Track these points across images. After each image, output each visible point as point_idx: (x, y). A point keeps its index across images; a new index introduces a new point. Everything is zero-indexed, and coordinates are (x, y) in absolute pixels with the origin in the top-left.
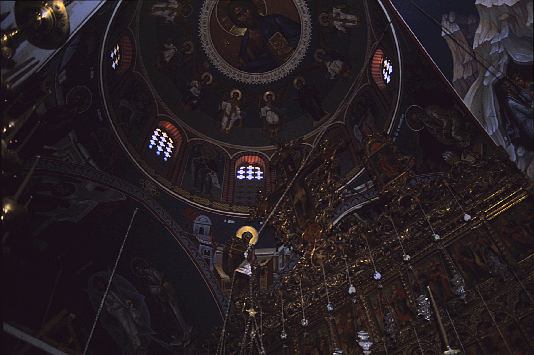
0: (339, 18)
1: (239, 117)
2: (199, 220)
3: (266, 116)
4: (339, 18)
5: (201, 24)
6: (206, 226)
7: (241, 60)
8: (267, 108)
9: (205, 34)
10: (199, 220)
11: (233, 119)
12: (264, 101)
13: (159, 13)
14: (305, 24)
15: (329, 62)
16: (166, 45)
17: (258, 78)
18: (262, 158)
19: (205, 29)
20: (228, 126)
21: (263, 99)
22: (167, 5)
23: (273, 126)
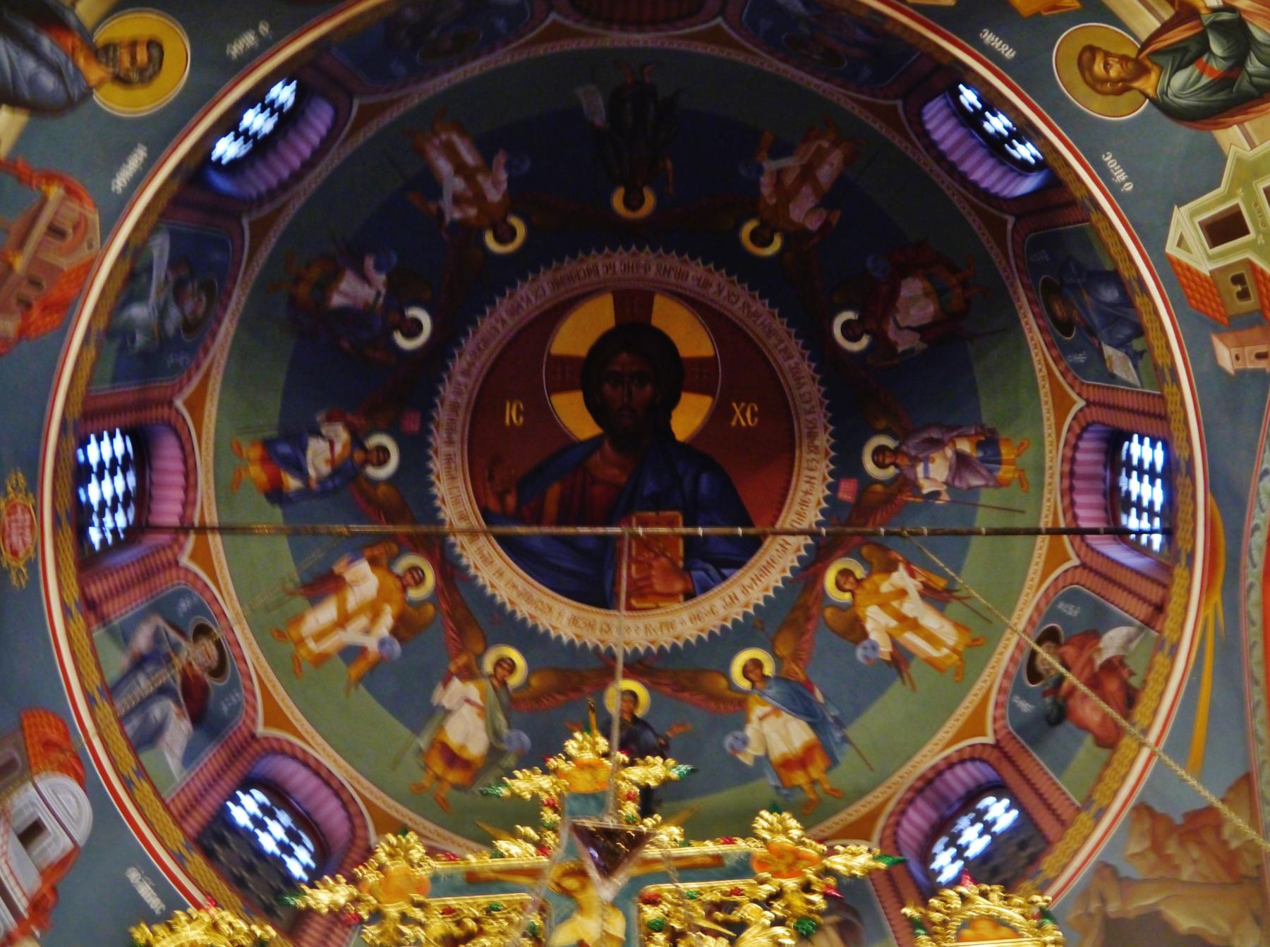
0: (895, 604)
3: (448, 713)
4: (895, 604)
5: (503, 306)
7: (511, 501)
8: (473, 691)
9: (486, 342)
11: (352, 635)
13: (444, 166)
14: (774, 553)
15: (767, 709)
16: (369, 262)
17: (514, 586)
19: (499, 326)
20: (320, 636)
21: (479, 658)
22: (477, 170)
23: (452, 758)
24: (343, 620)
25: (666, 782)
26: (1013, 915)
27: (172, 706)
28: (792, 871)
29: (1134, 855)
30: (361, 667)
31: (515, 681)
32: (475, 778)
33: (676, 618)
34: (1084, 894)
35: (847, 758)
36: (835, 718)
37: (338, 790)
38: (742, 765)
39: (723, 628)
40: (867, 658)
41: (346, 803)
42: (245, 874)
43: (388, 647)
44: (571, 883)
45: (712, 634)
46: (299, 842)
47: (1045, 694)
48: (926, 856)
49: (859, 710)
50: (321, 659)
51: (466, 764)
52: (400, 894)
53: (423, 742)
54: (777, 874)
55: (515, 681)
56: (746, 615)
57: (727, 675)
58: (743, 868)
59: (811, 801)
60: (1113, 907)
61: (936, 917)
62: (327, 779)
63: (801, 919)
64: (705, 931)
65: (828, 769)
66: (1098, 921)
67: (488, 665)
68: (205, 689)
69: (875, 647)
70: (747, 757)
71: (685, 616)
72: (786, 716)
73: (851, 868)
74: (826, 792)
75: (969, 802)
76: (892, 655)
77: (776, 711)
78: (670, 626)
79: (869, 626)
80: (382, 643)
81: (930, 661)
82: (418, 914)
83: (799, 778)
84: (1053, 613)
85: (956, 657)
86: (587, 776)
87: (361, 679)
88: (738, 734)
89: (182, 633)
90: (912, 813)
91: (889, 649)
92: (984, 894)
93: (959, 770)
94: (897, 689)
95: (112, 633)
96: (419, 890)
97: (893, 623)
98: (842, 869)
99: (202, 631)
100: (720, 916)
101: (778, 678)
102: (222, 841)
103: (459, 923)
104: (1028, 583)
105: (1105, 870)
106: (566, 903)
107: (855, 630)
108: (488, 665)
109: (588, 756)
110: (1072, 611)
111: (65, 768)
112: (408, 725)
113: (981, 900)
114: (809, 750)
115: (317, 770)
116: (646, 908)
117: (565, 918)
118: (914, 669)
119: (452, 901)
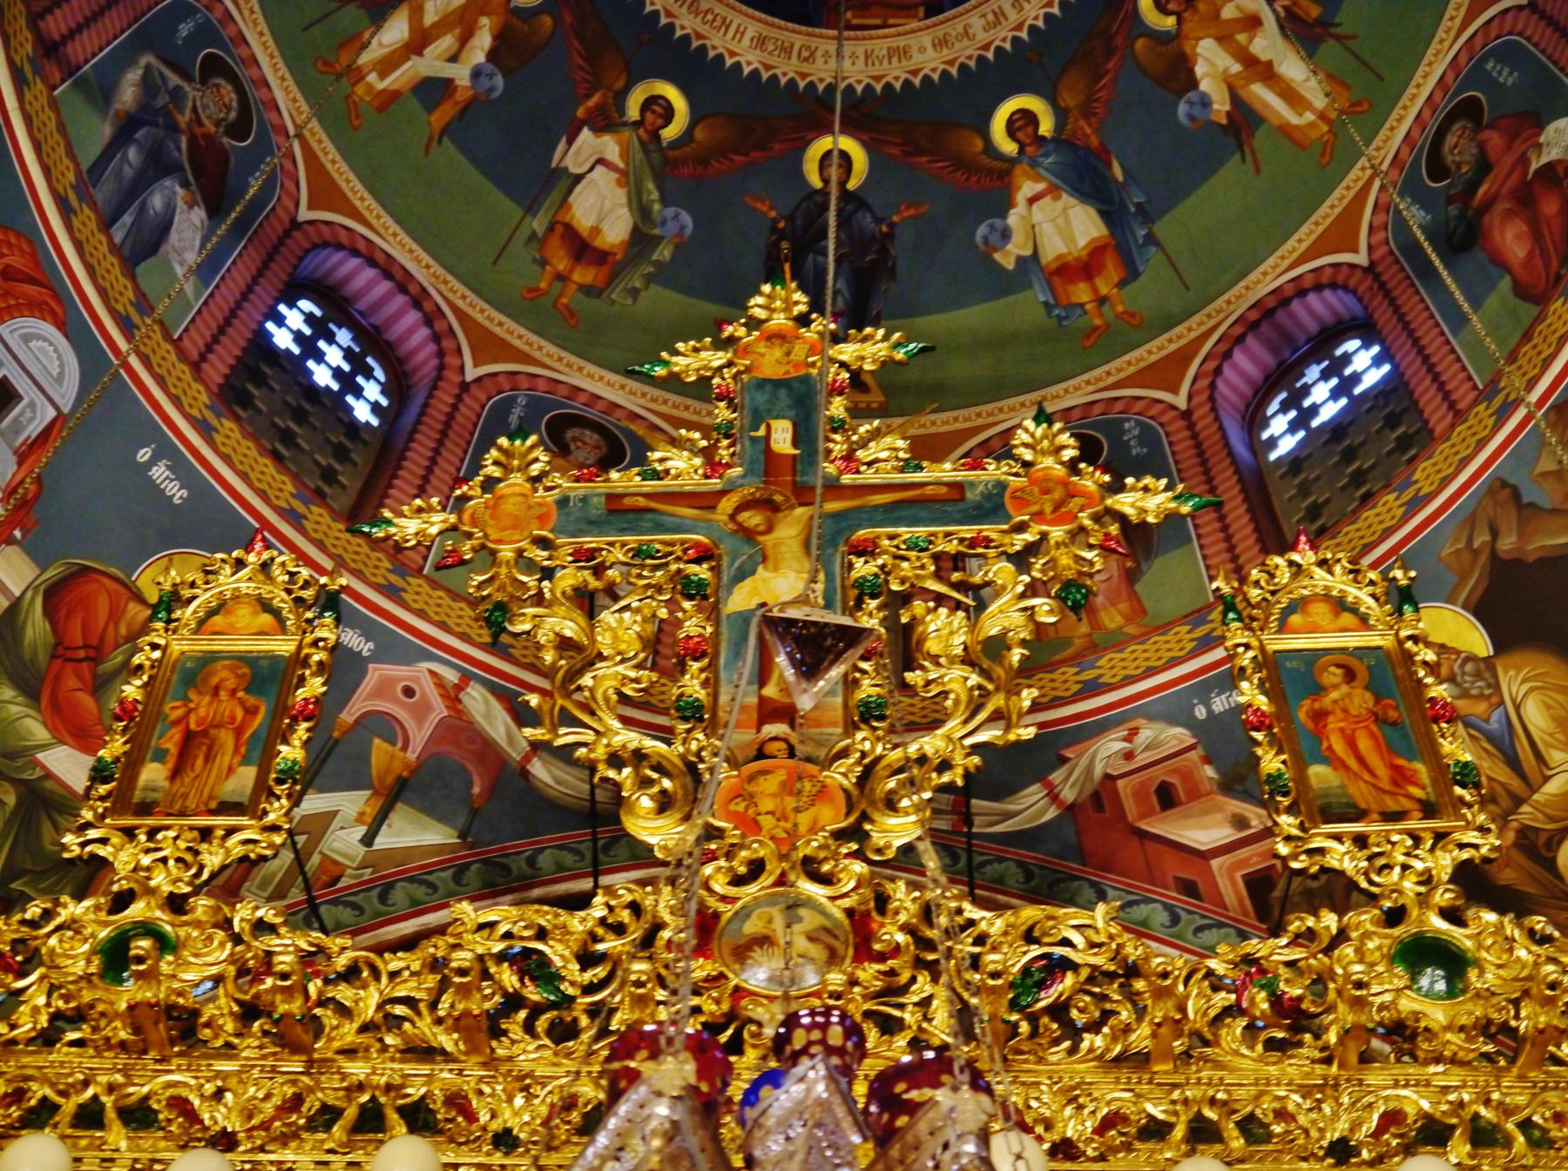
0: (1242, 38)
1: (461, 74)
2: (26, 339)
3: (579, 178)
6: (40, 399)
8: (610, 146)
10: (26, 339)
11: (431, 63)
12: (622, 110)
15: (1041, 186)
18: (436, 338)
20: (387, 65)
21: (621, 96)
23: (582, 248)
24: (418, 43)
25: (887, 364)
26: (1362, 596)
27: (180, 191)
28: (1060, 513)
29: (1544, 474)
30: (443, 115)
31: (670, 132)
32: (611, 281)
33: (911, 41)
34: (1471, 522)
35: (1153, 267)
36: (1138, 205)
37: (419, 299)
38: (999, 268)
39: (981, 60)
40: (1192, 118)
41: (431, 317)
42: (292, 425)
43: (485, 83)
44: (752, 519)
45: (963, 68)
46: (369, 374)
47: (1450, 200)
48: (1254, 419)
49: (1173, 197)
50: (390, 98)
51: (601, 257)
52: (517, 524)
53: (538, 224)
54: (1038, 516)
55: (670, 132)
56: (1016, 41)
57: (985, 133)
58: (992, 506)
59: (1096, 328)
60: (1507, 543)
61: (1254, 594)
62: (402, 281)
63: (1068, 585)
64: (940, 599)
65: (1122, 284)
66: (1484, 558)
67: (633, 111)
68: (223, 154)
69: (1205, 102)
70: (1007, 258)
71: (926, 39)
72: (1067, 199)
73: (1144, 511)
74: (1117, 316)
75: (1323, 344)
76: (1228, 114)
77: (1053, 191)
78: (904, 53)
79: (1200, 70)
80: (476, 73)
81: (1285, 130)
82: (539, 555)
83: (1081, 293)
84: (1477, 76)
85: (1325, 128)
86: (777, 353)
87: (443, 131)
88: (997, 222)
89: (186, 75)
90: (1239, 357)
91: (1227, 107)
92: (1322, 563)
93: (1312, 299)
94: (1233, 170)
95: (81, 85)
96: (542, 519)
97: (1236, 68)
98: (1129, 511)
99: (214, 67)
100: (956, 576)
101: (1060, 140)
102: (261, 381)
103: (598, 571)
104: (1445, 23)
105: (1504, 492)
106: (748, 550)
107: (1180, 75)
108: (633, 111)
109: (780, 321)
110: (1506, 76)
111: (35, 308)
112: (517, 200)
113: (1319, 573)
114: (1097, 252)
115: (388, 268)
116: (859, 562)
117: (742, 575)
118: (1261, 140)
119: (590, 541)
